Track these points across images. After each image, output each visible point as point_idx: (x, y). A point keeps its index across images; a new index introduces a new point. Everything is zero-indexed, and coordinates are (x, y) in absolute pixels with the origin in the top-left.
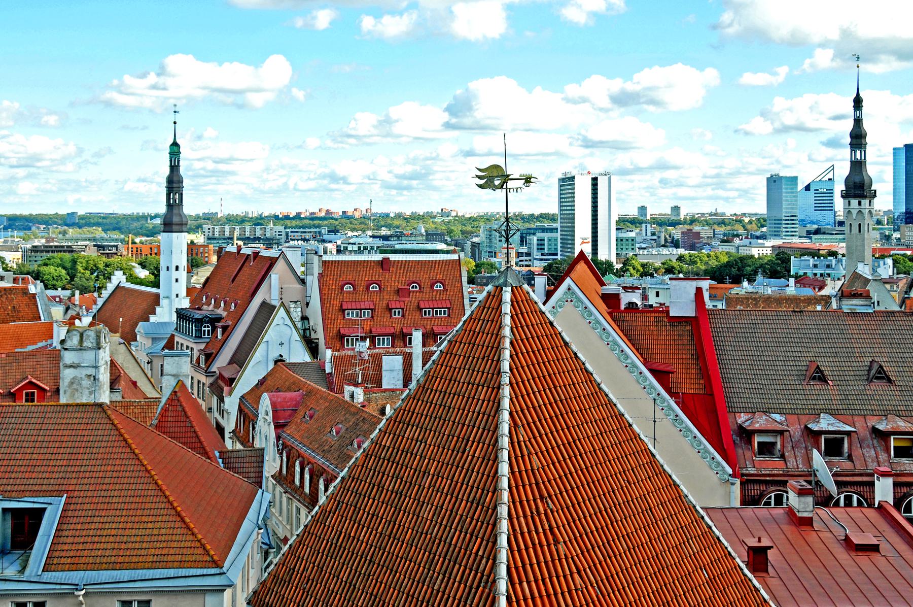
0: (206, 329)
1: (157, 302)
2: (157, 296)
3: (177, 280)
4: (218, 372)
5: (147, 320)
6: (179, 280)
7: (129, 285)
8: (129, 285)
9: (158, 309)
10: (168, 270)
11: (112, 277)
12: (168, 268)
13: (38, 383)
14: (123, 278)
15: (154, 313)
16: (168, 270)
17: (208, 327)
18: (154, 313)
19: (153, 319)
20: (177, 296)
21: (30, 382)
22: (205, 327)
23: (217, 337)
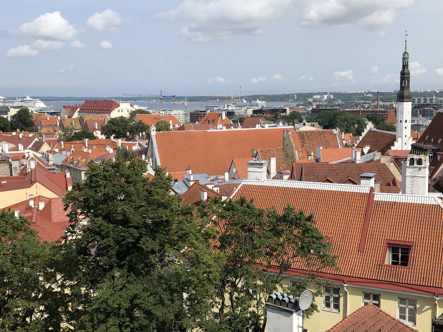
0: (431, 155)
1: (395, 140)
2: (395, 136)
3: (406, 128)
4: (438, 179)
5: (390, 149)
6: (407, 128)
7: (375, 130)
8: (375, 130)
9: (396, 143)
10: (401, 122)
11: (367, 126)
12: (401, 121)
13: (352, 179)
14: (372, 126)
15: (393, 145)
16: (401, 122)
17: (431, 154)
18: (393, 145)
19: (393, 148)
20: (406, 136)
21: (349, 179)
22: (429, 154)
23: (437, 159)
